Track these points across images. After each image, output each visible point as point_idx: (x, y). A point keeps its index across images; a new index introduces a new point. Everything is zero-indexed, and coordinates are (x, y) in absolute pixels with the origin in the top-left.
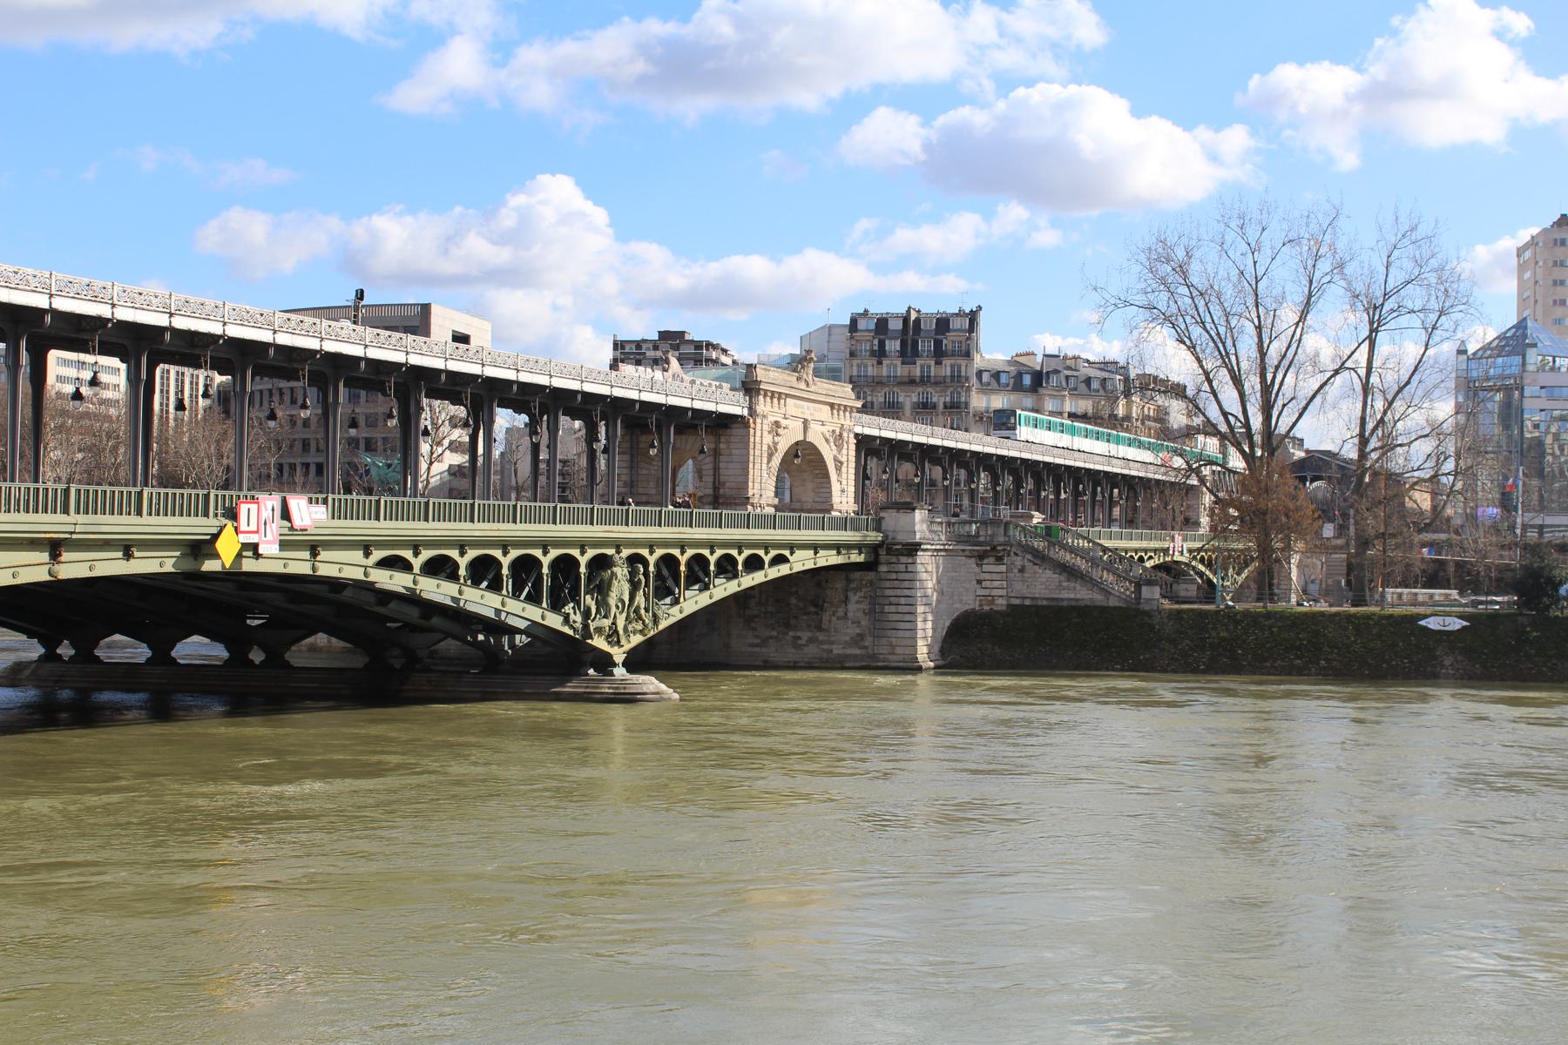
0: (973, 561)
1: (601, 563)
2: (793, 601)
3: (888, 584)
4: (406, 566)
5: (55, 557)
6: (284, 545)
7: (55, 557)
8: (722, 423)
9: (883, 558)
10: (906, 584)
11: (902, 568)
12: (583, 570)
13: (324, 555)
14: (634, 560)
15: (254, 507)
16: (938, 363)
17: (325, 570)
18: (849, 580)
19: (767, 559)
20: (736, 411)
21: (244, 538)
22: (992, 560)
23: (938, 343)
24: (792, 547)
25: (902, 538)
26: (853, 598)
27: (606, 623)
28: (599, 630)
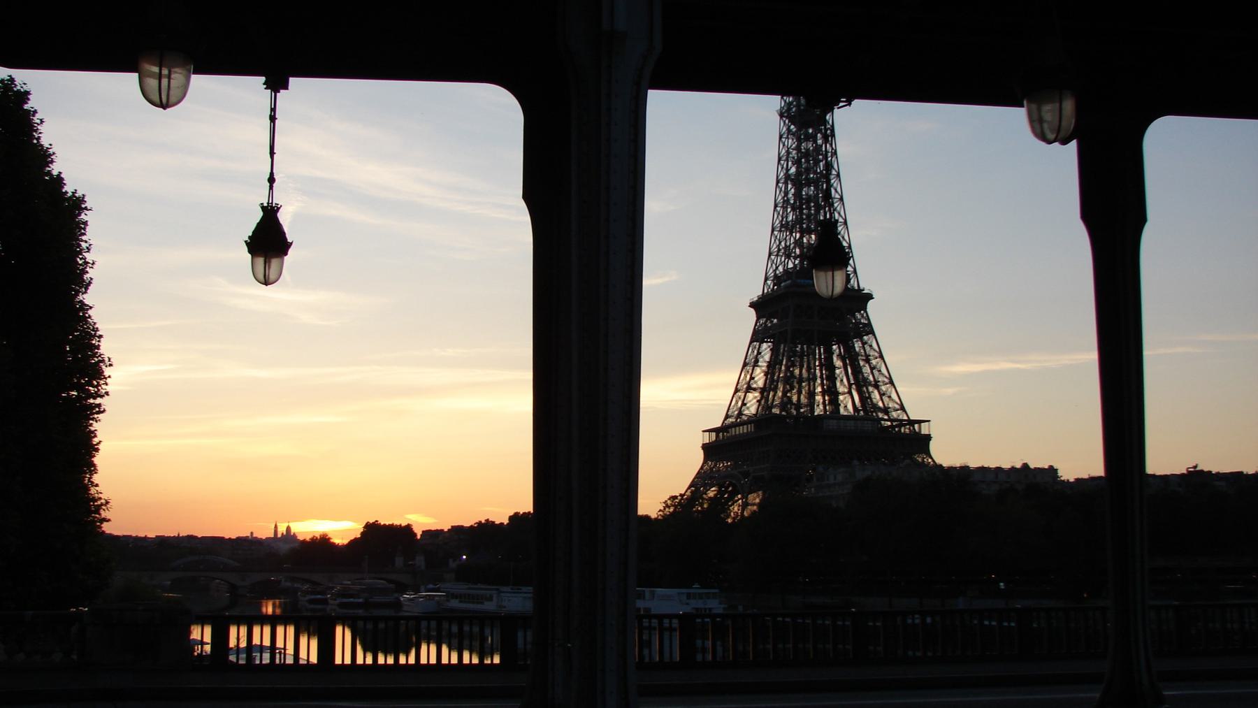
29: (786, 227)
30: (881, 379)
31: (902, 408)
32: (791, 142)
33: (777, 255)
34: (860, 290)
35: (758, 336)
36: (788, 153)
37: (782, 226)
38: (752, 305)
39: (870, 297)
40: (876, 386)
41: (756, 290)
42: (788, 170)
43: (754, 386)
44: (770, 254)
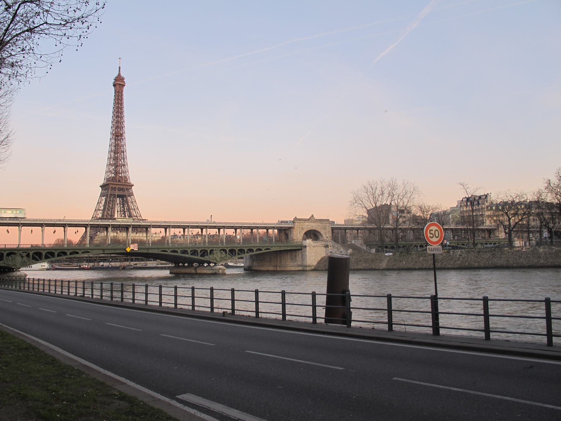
0: (324, 248)
1: (211, 251)
2: (293, 256)
3: (303, 252)
4: (167, 251)
5: (104, 251)
6: (138, 249)
7: (104, 251)
8: (290, 228)
9: (303, 248)
10: (306, 252)
11: (305, 249)
12: (209, 252)
13: (149, 250)
14: (220, 250)
15: (133, 245)
16: (478, 206)
17: (149, 252)
18: (299, 252)
19: (263, 249)
20: (291, 226)
21: (131, 249)
22: (327, 247)
23: (478, 202)
24: (272, 247)
25: (305, 245)
26: (300, 255)
27: (214, 258)
28: (213, 259)
29: (110, 164)
30: (135, 208)
31: (141, 216)
32: (113, 141)
33: (108, 173)
34: (130, 183)
35: (102, 195)
36: (112, 144)
37: (109, 165)
38: (101, 187)
39: (133, 185)
40: (134, 210)
41: (102, 182)
42: (112, 149)
43: (101, 209)
44: (106, 172)
